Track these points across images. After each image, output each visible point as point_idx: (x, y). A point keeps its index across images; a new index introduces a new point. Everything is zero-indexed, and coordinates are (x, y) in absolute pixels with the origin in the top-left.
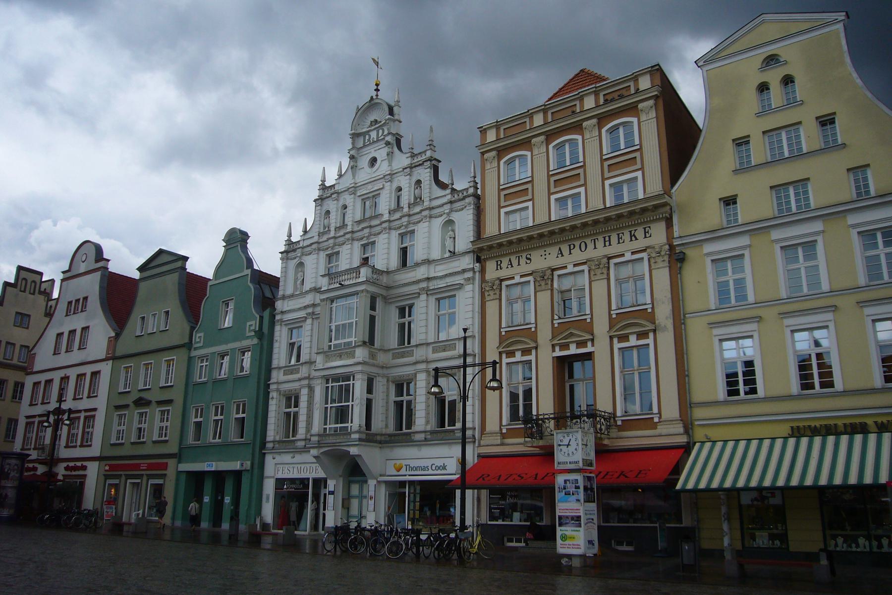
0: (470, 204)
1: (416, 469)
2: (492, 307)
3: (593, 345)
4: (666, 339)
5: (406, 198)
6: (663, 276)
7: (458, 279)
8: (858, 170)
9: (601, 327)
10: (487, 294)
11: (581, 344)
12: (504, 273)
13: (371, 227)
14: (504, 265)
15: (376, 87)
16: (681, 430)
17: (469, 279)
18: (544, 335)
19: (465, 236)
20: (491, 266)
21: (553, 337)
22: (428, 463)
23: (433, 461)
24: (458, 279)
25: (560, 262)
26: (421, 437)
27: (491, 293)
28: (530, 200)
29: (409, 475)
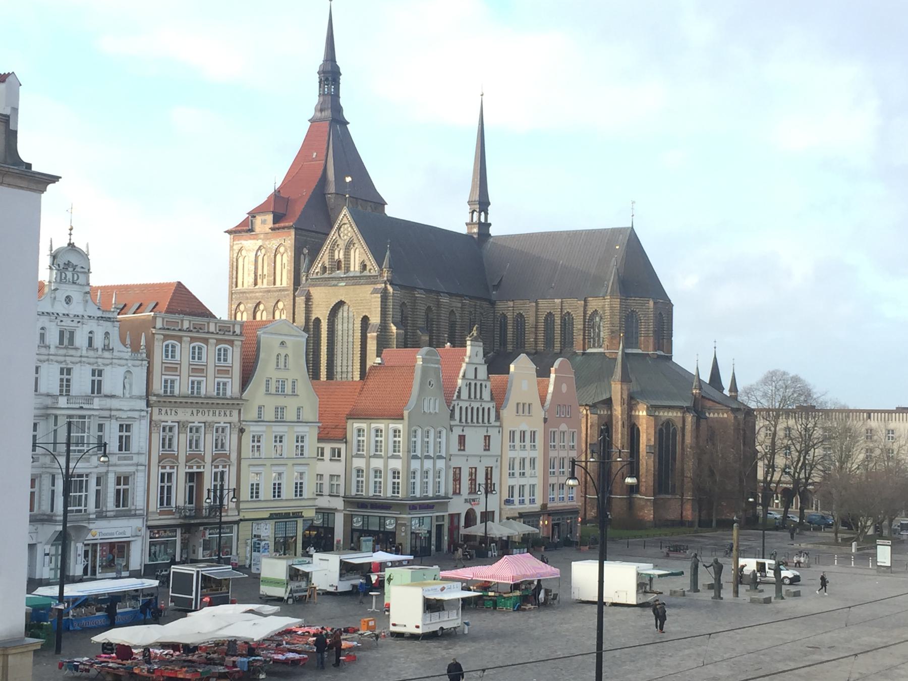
0: (145, 365)
1: (106, 534)
2: (155, 437)
3: (204, 468)
4: (234, 469)
5: (98, 342)
6: (235, 437)
7: (136, 414)
9: (208, 459)
10: (153, 428)
11: (199, 467)
12: (163, 418)
13: (72, 356)
14: (163, 412)
15: (69, 232)
16: (237, 514)
17: (143, 416)
18: (182, 459)
19: (139, 388)
20: (156, 410)
21: (186, 462)
22: (114, 531)
23: (117, 529)
24: (136, 414)
25: (191, 419)
26: (112, 514)
27: (156, 428)
28: (178, 375)
29: (101, 539)
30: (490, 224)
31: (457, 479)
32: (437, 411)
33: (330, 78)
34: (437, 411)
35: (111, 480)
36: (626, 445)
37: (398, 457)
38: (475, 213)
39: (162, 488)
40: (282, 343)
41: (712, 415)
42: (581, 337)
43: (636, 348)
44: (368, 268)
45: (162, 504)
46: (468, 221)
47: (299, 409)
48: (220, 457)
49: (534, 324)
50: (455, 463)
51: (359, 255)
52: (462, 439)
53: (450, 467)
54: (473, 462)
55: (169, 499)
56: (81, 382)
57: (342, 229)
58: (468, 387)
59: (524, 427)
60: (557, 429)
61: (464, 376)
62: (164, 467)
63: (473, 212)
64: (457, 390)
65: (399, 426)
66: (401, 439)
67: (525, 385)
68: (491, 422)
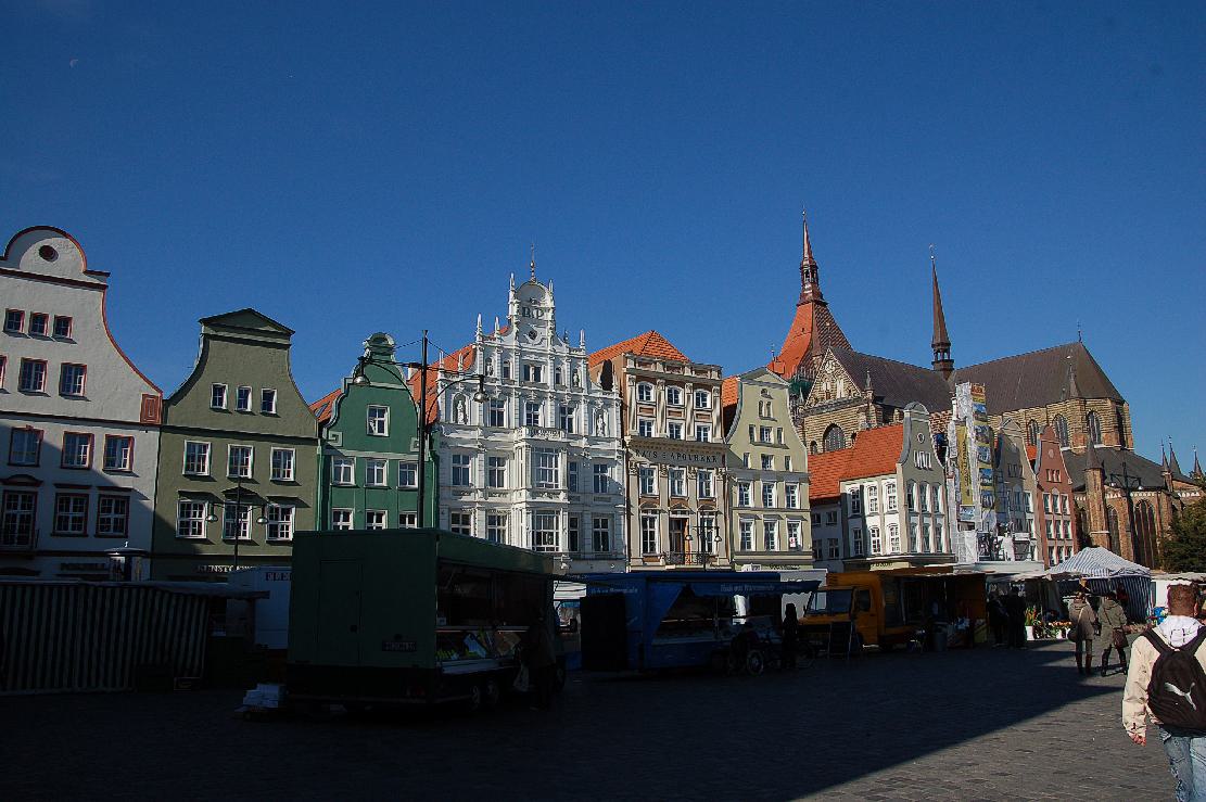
18: (663, 505)
30: (952, 361)
35: (588, 519)
37: (895, 512)
39: (645, 533)
40: (763, 391)
41: (1184, 495)
45: (645, 550)
47: (787, 458)
48: (706, 504)
51: (843, 389)
55: (653, 544)
56: (547, 415)
62: (646, 512)
66: (895, 494)
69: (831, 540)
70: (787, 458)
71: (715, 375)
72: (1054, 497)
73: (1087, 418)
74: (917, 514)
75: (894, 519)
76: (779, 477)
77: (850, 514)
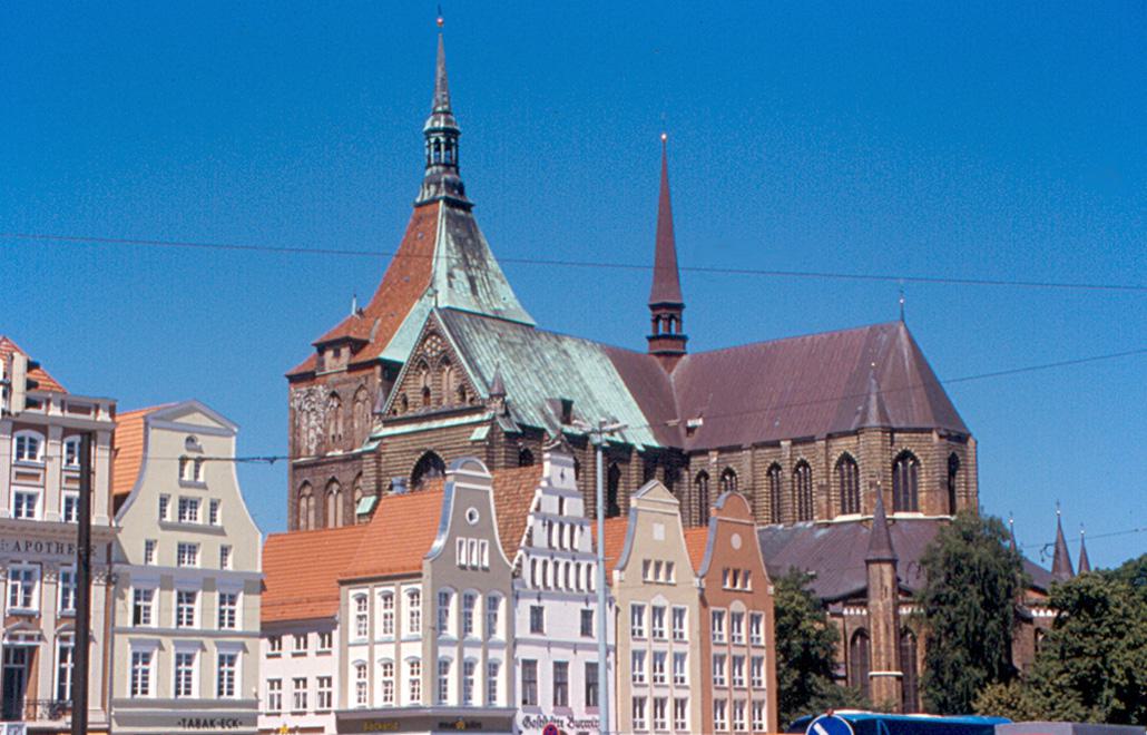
8: (225, 551)
30: (684, 339)
31: (530, 682)
32: (486, 563)
33: (442, 139)
34: (486, 563)
36: (893, 664)
38: (661, 322)
40: (190, 440)
42: (824, 497)
43: (915, 509)
44: (468, 397)
46: (651, 333)
49: (750, 482)
50: (523, 653)
52: (537, 613)
53: (516, 662)
54: (561, 655)
57: (428, 342)
58: (546, 527)
59: (659, 601)
60: (725, 609)
61: (538, 509)
63: (656, 320)
64: (527, 531)
65: (419, 587)
67: (659, 532)
68: (593, 587)
69: (321, 680)
70: (225, 551)
71: (104, 416)
72: (737, 618)
73: (895, 467)
74: (450, 643)
75: (416, 650)
76: (209, 582)
77: (353, 637)
